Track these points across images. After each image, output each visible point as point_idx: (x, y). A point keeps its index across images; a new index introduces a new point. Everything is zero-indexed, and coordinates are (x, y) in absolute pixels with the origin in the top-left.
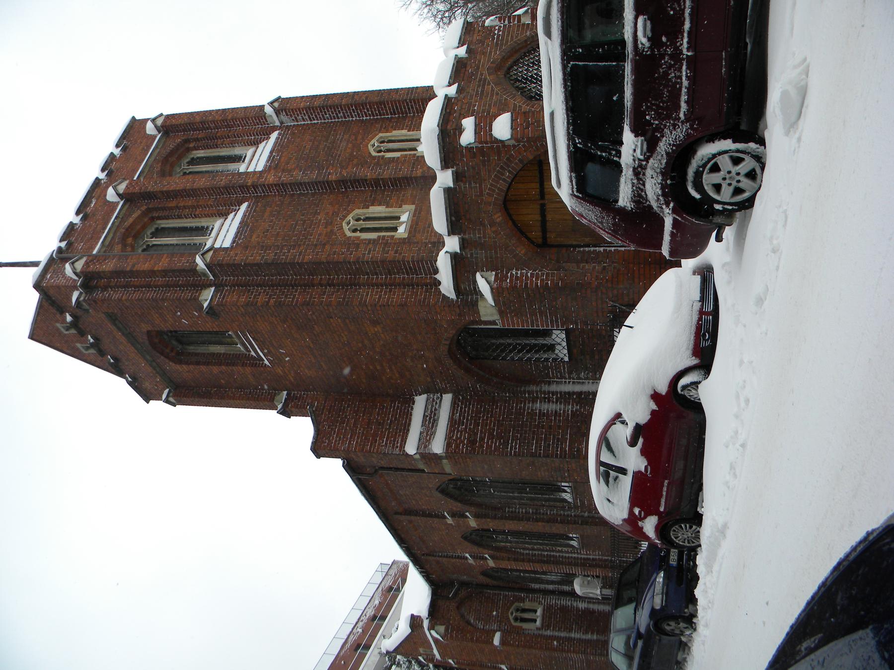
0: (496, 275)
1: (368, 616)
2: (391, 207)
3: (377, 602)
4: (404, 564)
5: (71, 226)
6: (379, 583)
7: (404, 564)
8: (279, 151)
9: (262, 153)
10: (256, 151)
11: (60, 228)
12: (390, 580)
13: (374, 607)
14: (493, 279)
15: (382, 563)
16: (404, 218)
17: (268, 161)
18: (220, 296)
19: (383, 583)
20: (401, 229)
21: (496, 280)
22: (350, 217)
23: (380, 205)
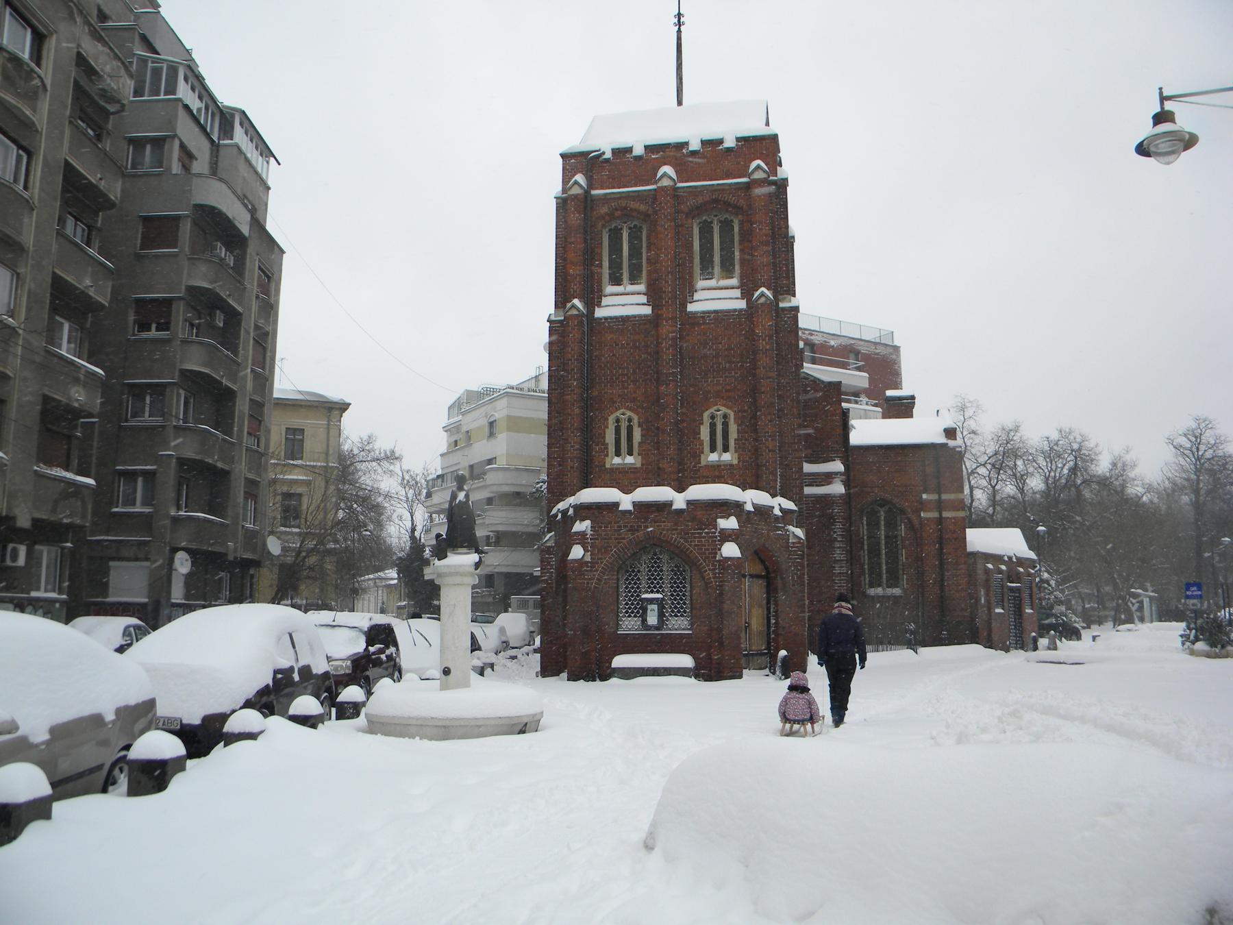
0: (552, 547)
1: (812, 337)
2: (639, 447)
3: (832, 343)
4: (895, 360)
5: (629, 150)
6: (863, 338)
7: (895, 360)
8: (715, 319)
9: (723, 299)
10: (733, 288)
11: (622, 141)
12: (868, 349)
13: (825, 341)
14: (548, 545)
15: (894, 334)
16: (630, 460)
17: (704, 312)
18: (558, 327)
19: (863, 343)
20: (617, 460)
21: (546, 547)
22: (629, 413)
23: (642, 436)
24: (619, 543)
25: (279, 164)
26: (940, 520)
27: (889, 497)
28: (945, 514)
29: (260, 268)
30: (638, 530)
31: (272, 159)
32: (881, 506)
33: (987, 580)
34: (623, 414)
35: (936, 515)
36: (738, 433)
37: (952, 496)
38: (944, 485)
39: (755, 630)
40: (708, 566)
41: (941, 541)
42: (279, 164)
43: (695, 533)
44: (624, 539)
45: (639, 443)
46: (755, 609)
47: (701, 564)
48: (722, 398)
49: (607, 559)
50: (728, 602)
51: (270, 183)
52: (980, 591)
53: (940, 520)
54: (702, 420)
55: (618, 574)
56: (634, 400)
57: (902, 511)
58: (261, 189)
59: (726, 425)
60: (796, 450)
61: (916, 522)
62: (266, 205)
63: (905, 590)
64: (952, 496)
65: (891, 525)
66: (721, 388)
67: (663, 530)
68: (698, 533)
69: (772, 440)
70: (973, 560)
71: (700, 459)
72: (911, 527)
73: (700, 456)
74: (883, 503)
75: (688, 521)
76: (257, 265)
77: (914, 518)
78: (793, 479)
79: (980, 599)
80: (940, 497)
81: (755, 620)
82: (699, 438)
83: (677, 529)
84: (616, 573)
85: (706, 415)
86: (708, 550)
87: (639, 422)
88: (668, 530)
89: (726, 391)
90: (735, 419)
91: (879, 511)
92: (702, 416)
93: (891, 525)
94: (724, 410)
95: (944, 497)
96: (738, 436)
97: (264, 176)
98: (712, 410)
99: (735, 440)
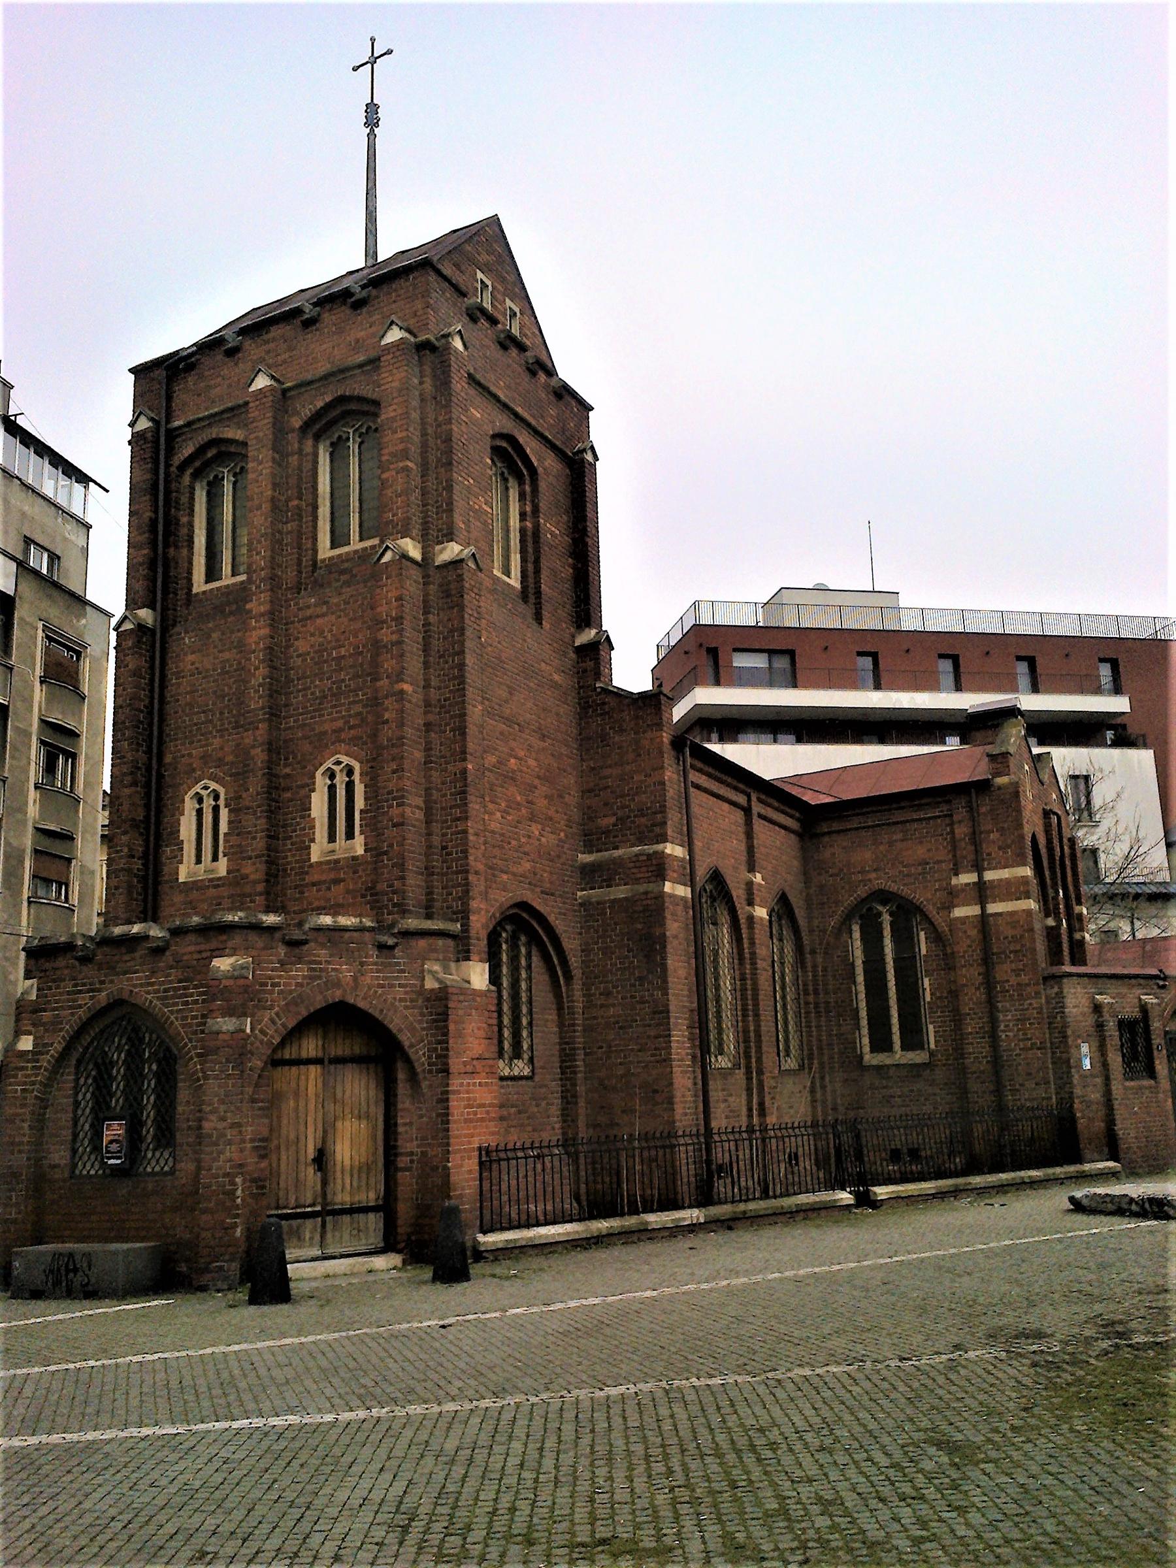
2: (226, 841)
22: (213, 785)
23: (230, 822)
24: (72, 1014)
25: (107, 491)
26: (984, 915)
27: (894, 888)
28: (992, 908)
29: (48, 637)
30: (99, 990)
31: (91, 484)
32: (884, 904)
33: (1100, 1026)
34: (206, 788)
35: (973, 910)
36: (366, 799)
37: (1005, 874)
38: (989, 854)
39: (347, 1162)
40: (195, 1048)
41: (987, 961)
42: (107, 491)
43: (179, 988)
44: (80, 1006)
45: (225, 834)
46: (347, 1124)
47: (186, 1045)
48: (343, 741)
49: (58, 1046)
50: (213, 1118)
51: (89, 519)
52: (1078, 1047)
53: (984, 917)
54: (314, 783)
55: (76, 1074)
56: (220, 762)
57: (919, 910)
58: (68, 527)
59: (350, 786)
60: (458, 819)
61: (943, 927)
62: (85, 551)
63: (932, 1054)
64: (1005, 874)
65: (904, 939)
66: (340, 723)
67: (135, 986)
68: (185, 988)
69: (398, 805)
70: (1056, 989)
71: (309, 854)
72: (937, 937)
73: (309, 847)
74: (884, 896)
75: (171, 967)
76: (40, 633)
77: (938, 919)
78: (453, 873)
79: (1079, 1065)
80: (980, 877)
81: (347, 1143)
82: (309, 815)
83: (152, 984)
84: (72, 1070)
85: (319, 773)
86: (195, 1017)
87: (226, 799)
88: (141, 985)
89: (351, 728)
90: (361, 775)
91: (880, 914)
92: (314, 777)
93: (904, 939)
94: (345, 760)
95: (989, 876)
96: (366, 805)
97: (77, 510)
98: (329, 764)
99: (361, 811)
